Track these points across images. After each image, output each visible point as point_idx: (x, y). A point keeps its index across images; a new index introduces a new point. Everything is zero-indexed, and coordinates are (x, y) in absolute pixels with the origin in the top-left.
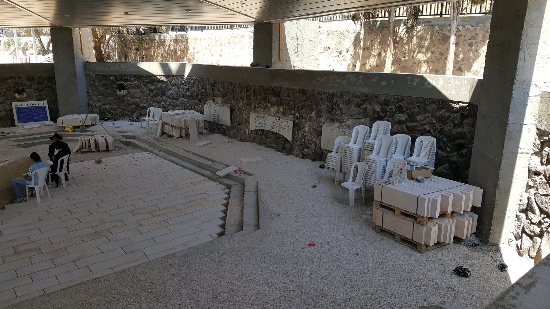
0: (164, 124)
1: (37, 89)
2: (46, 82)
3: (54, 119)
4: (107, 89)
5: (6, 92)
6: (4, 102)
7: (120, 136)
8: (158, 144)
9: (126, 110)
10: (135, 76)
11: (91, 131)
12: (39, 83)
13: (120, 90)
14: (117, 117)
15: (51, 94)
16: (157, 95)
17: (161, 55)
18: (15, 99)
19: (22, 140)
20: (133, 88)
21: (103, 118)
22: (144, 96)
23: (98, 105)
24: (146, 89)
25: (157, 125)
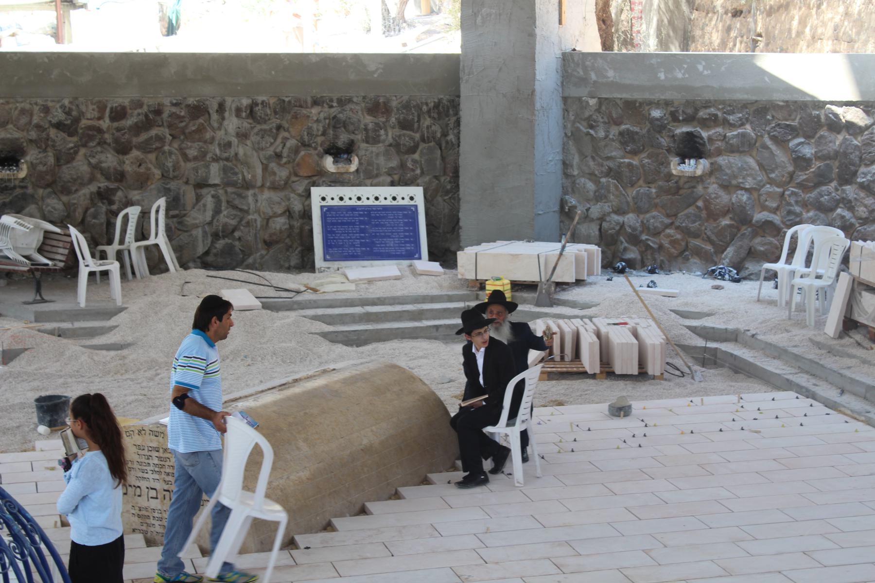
0: (859, 286)
1: (396, 145)
2: (427, 122)
3: (444, 254)
4: (634, 153)
5: (296, 151)
6: (286, 185)
7: (680, 328)
8: (835, 367)
9: (696, 236)
10: (745, 105)
11: (573, 305)
12: (405, 125)
13: (683, 157)
14: (660, 257)
15: (438, 162)
16: (822, 179)
17: (829, 31)
18: (320, 177)
19: (342, 319)
20: (732, 150)
21: (613, 264)
22: (771, 182)
23: (596, 210)
24: (781, 156)
25: (824, 294)
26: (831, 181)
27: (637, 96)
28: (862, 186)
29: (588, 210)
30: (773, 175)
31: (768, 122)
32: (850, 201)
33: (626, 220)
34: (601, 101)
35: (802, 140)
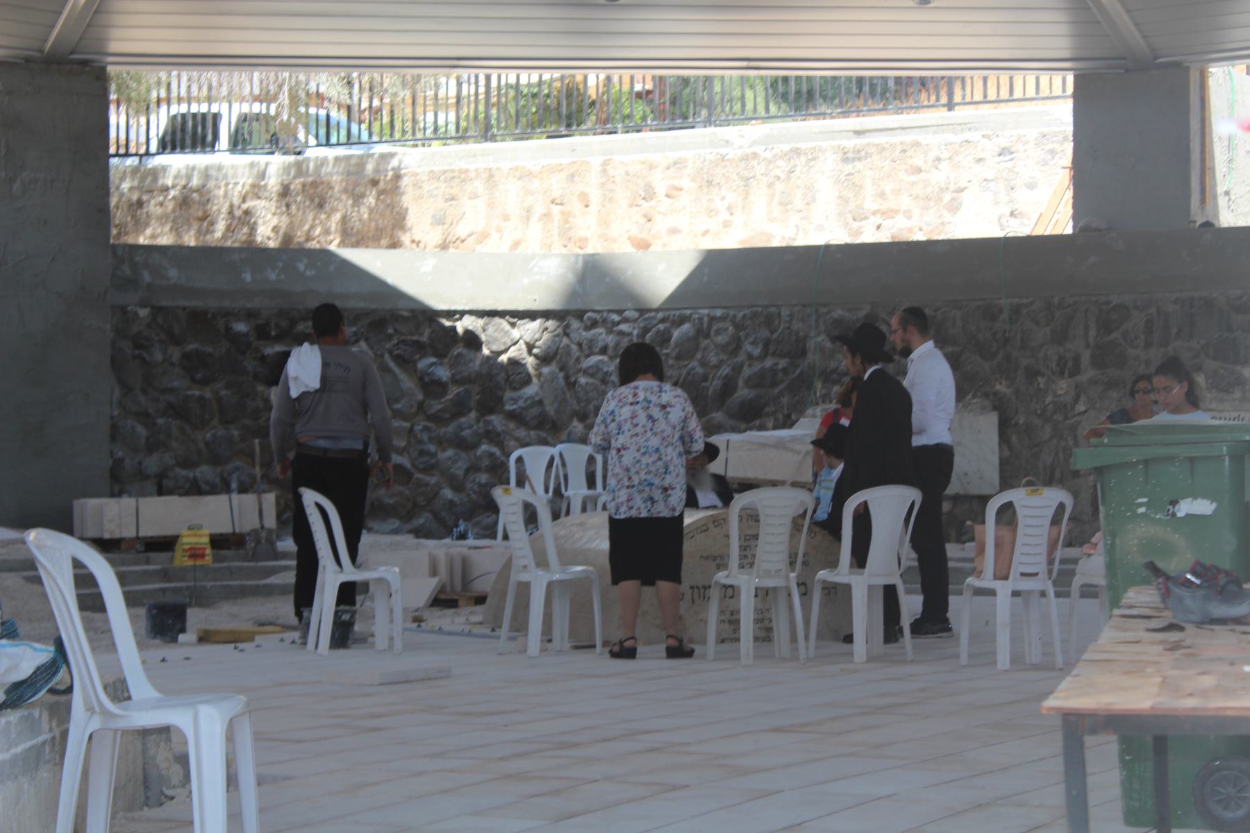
4: (204, 383)
10: (358, 316)
16: (460, 407)
26: (470, 411)
27: (212, 304)
28: (512, 416)
29: (140, 463)
30: (398, 406)
31: (390, 337)
32: (498, 435)
33: (198, 474)
34: (157, 310)
35: (433, 360)
